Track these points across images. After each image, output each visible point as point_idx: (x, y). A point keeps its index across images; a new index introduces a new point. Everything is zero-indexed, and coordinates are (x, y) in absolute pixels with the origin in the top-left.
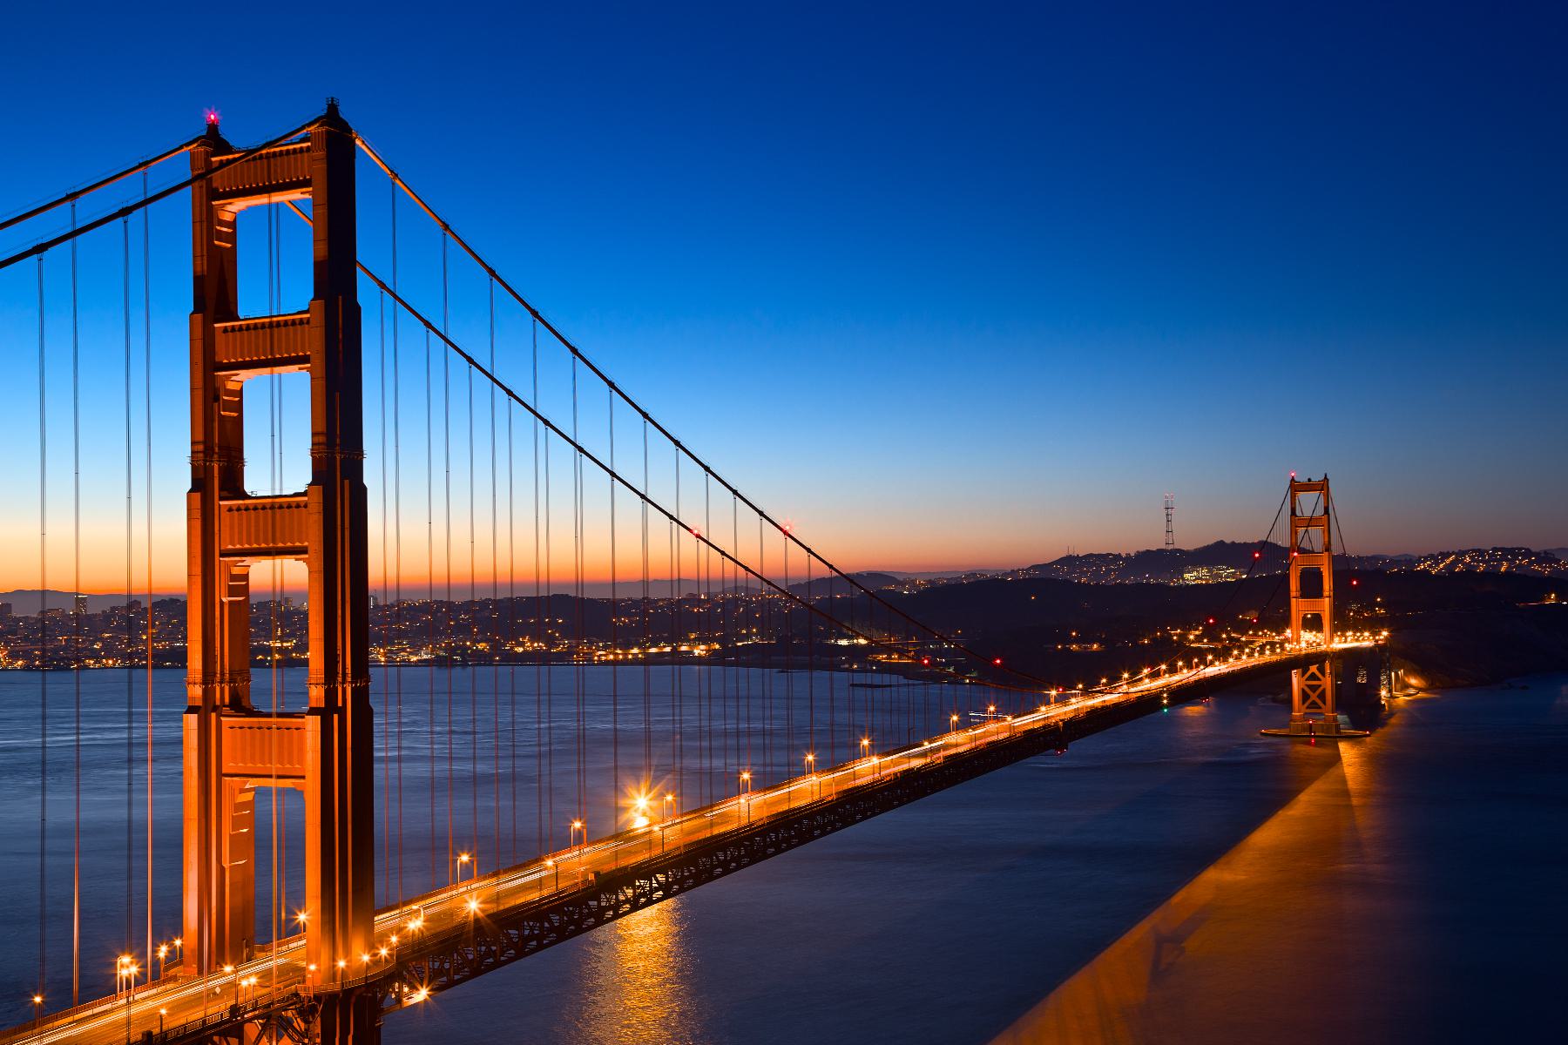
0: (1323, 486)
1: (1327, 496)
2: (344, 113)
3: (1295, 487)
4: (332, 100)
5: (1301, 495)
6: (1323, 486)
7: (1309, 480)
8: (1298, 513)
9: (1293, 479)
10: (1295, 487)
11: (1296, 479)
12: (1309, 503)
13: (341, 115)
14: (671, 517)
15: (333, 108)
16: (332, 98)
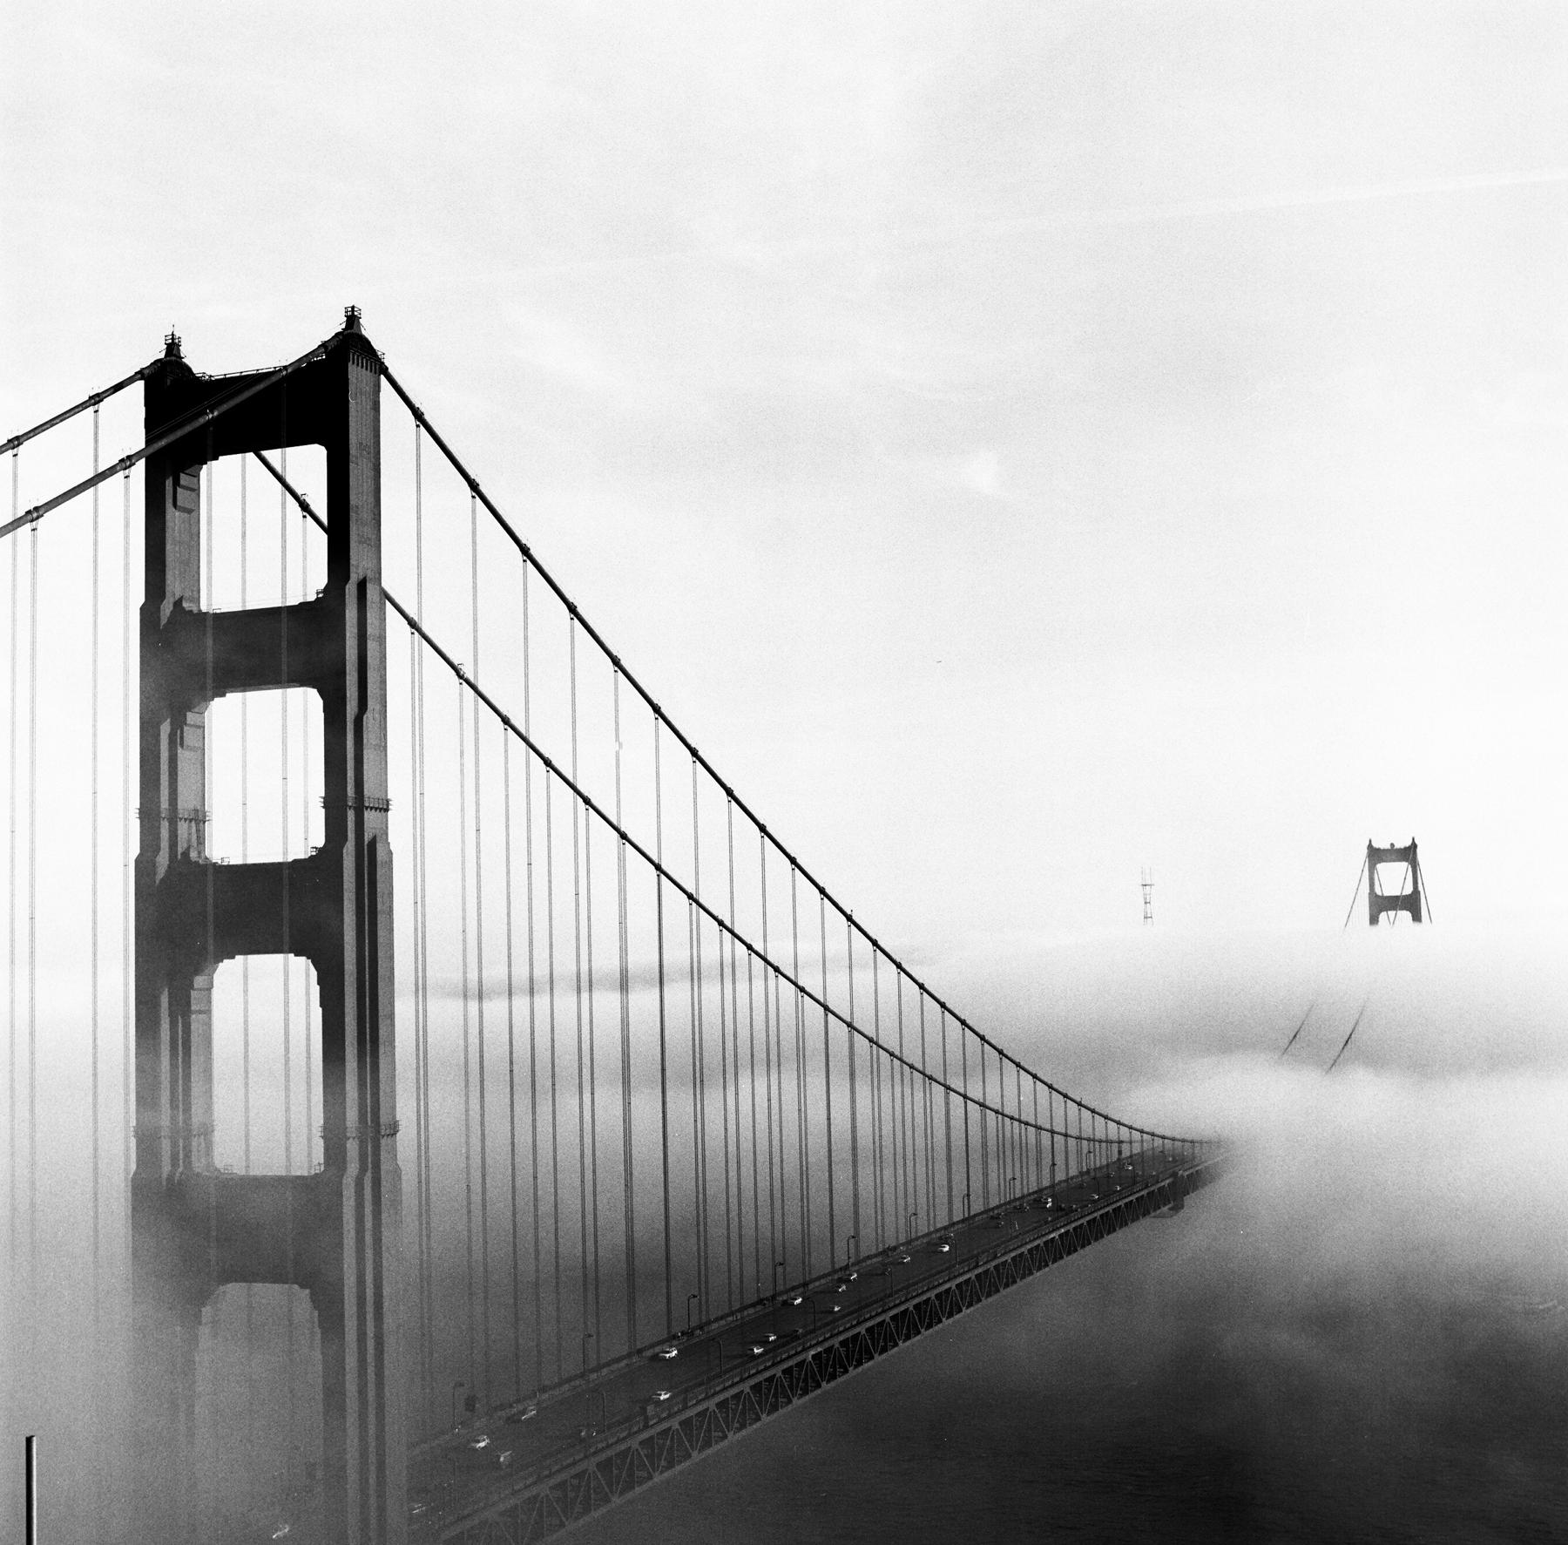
0: (1408, 854)
1: (1414, 865)
2: (370, 329)
3: (1376, 855)
4: (353, 307)
5: (1381, 867)
6: (1408, 854)
7: (1392, 845)
8: (1379, 893)
9: (1370, 846)
10: (1376, 855)
11: (1375, 845)
12: (1393, 879)
13: (364, 332)
14: (690, 897)
15: (352, 319)
16: (353, 307)
